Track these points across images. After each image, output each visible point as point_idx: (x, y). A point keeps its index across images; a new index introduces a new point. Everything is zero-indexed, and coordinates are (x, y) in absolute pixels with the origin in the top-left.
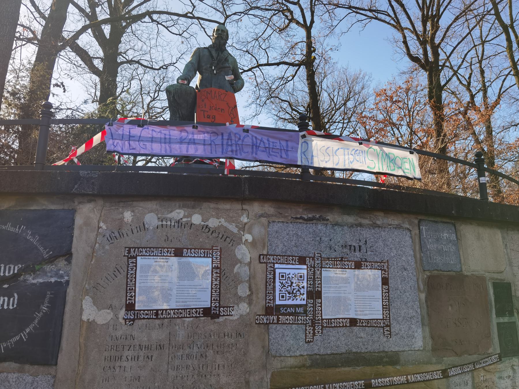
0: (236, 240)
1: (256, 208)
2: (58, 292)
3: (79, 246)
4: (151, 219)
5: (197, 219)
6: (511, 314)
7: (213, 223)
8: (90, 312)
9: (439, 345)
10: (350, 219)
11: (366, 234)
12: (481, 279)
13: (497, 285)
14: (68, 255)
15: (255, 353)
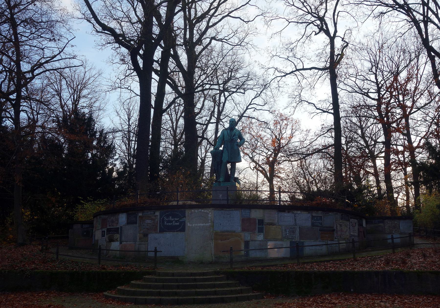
0: (208, 214)
1: (211, 209)
2: (184, 222)
3: (187, 215)
4: (196, 211)
5: (203, 211)
6: (263, 225)
7: (205, 211)
8: (189, 225)
9: (243, 230)
10: (228, 209)
11: (231, 212)
12: (255, 219)
13: (259, 220)
14: (185, 217)
15: (212, 230)
